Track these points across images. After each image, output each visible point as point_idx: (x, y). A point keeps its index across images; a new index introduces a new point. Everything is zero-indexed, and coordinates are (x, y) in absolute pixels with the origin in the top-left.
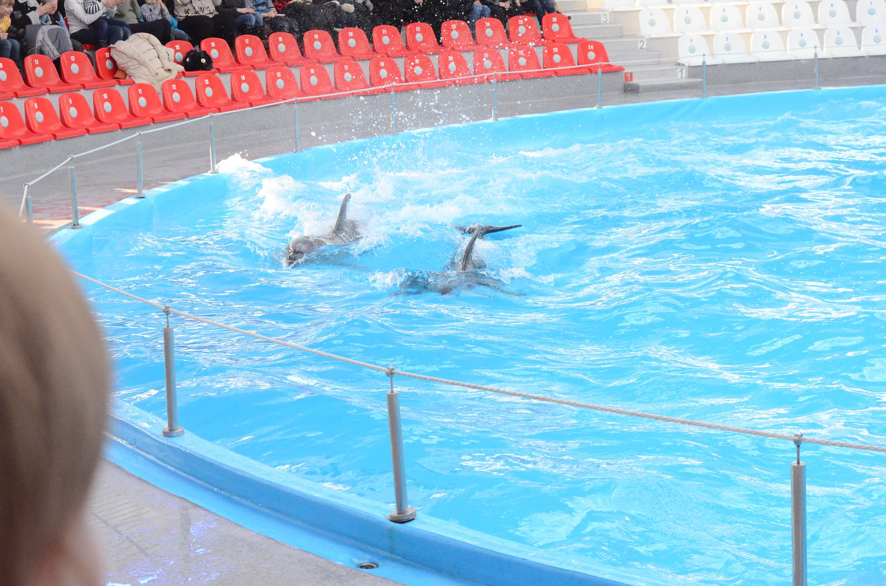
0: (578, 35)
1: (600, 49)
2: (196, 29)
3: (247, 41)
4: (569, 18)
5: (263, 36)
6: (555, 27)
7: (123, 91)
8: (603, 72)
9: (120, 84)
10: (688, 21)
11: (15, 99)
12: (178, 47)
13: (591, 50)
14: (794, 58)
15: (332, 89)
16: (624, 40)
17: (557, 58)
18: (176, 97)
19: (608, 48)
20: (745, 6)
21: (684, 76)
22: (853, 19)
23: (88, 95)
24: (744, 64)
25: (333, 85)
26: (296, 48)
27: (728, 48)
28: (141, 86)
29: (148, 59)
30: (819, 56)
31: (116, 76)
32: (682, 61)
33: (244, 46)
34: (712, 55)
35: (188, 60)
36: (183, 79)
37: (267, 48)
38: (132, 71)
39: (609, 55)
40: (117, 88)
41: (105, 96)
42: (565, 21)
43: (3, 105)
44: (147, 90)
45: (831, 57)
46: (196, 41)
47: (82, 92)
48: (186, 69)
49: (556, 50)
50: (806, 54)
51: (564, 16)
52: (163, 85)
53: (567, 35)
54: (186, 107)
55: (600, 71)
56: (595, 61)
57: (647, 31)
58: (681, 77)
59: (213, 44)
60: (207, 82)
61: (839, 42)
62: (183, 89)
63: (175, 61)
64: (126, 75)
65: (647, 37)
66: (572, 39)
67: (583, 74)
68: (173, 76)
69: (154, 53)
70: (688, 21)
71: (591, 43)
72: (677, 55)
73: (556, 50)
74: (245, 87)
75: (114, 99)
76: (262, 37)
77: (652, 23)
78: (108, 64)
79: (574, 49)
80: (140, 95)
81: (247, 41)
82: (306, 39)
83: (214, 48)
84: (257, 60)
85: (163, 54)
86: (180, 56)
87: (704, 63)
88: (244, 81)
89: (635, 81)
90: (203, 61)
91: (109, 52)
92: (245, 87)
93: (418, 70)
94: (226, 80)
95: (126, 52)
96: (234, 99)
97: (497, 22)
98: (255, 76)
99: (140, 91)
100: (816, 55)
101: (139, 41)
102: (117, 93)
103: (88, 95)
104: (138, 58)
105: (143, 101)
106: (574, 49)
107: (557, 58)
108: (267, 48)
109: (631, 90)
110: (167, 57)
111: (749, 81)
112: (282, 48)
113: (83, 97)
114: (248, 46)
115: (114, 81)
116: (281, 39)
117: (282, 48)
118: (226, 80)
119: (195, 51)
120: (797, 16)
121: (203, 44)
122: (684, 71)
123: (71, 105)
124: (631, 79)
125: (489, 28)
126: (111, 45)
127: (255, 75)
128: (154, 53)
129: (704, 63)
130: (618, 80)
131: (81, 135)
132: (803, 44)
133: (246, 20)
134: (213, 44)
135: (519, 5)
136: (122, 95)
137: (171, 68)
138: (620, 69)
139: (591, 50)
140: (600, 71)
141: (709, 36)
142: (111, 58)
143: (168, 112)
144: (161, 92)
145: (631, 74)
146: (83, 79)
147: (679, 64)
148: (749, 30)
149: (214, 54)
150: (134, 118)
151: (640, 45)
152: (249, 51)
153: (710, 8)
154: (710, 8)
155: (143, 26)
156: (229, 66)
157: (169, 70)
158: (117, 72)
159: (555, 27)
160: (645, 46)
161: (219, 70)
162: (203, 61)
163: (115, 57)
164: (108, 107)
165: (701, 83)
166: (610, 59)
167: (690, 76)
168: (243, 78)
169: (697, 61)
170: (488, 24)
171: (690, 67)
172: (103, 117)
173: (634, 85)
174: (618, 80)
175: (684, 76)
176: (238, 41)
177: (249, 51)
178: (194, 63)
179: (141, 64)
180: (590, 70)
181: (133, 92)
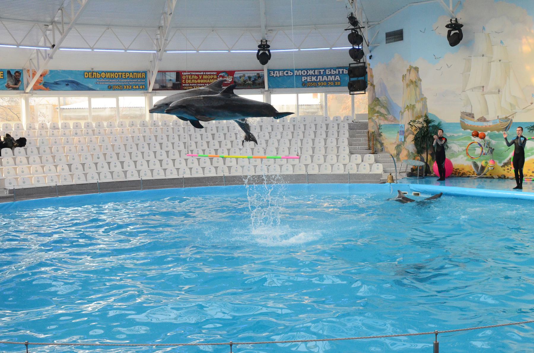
10: (9, 173)
22: (70, 171)
50: (53, 184)
58: (6, 194)
61: (65, 179)
70: (9, 173)
120: (50, 170)
132: (52, 180)
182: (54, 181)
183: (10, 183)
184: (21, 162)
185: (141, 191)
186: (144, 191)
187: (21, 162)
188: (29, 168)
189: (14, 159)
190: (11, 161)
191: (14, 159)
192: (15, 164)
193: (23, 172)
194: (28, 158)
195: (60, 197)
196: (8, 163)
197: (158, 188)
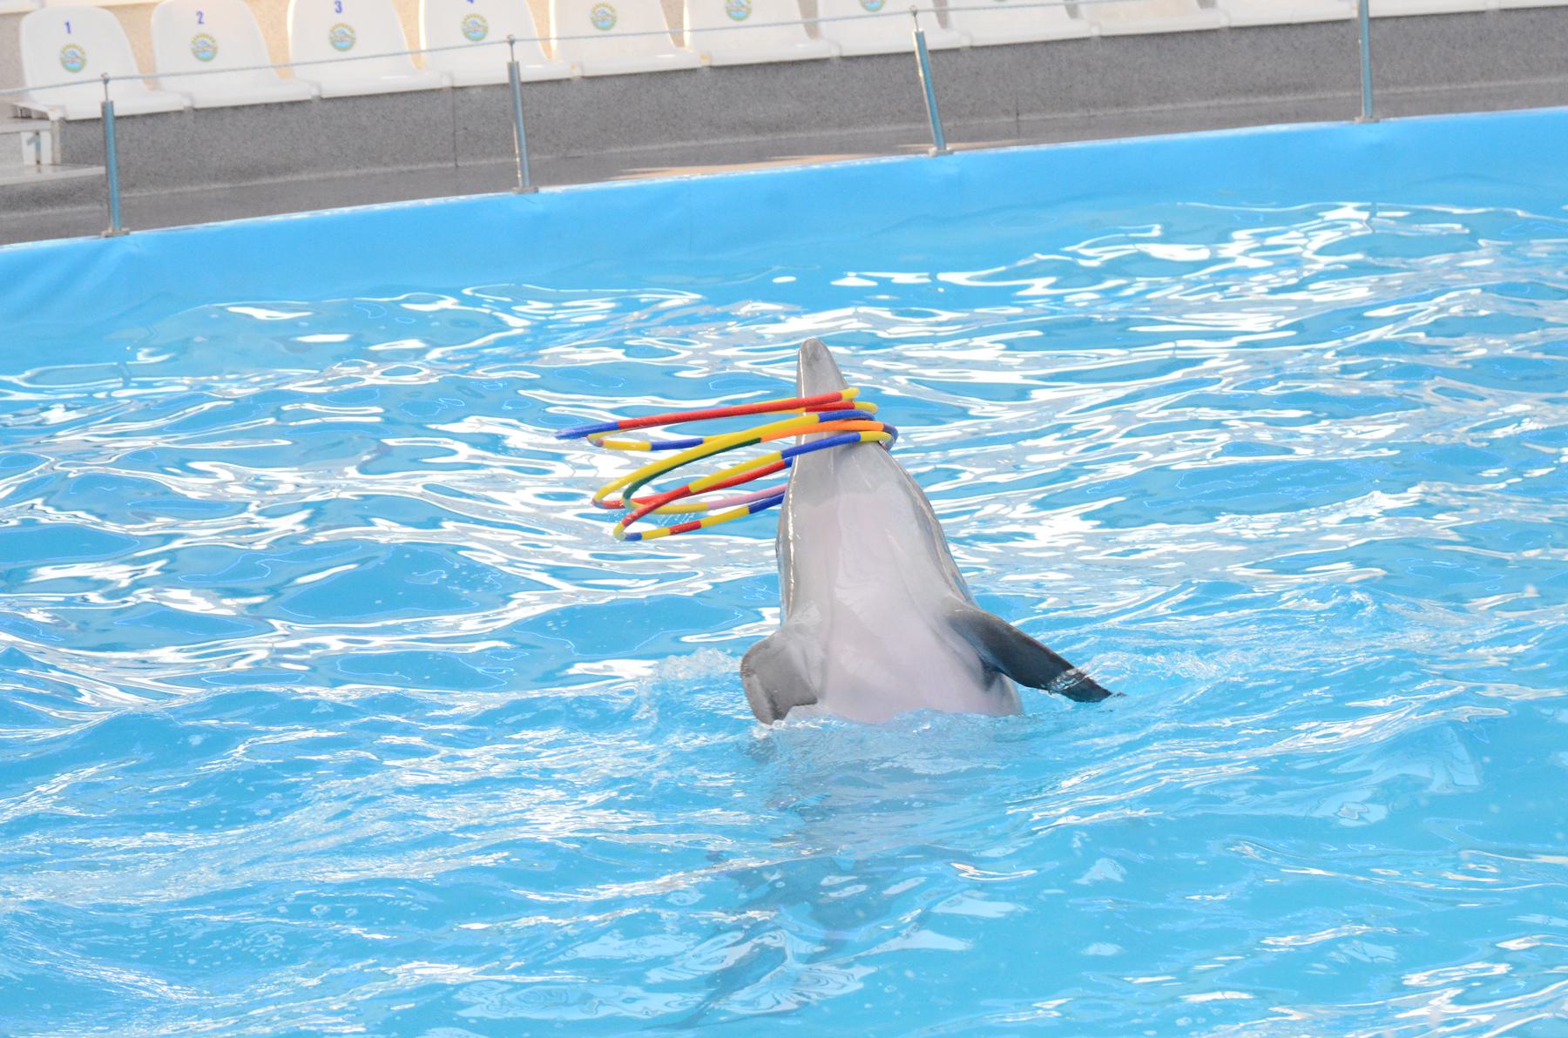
14: (446, 83)
21: (46, 158)
24: (267, 106)
27: (204, 50)
30: (530, 72)
32: (37, 102)
45: (576, 73)
58: (33, 161)
72: (19, 80)
87: (107, 107)
100: (513, 68)
111: (287, 169)
122: (46, 138)
129: (107, 107)
132: (475, 31)
147: (26, 115)
167: (71, 157)
171: (65, 122)
175: (46, 158)
182: (497, 32)
183: (73, 61)
185: (1362, 132)
186: (1391, 127)
195: (544, 190)
197: (1537, 100)
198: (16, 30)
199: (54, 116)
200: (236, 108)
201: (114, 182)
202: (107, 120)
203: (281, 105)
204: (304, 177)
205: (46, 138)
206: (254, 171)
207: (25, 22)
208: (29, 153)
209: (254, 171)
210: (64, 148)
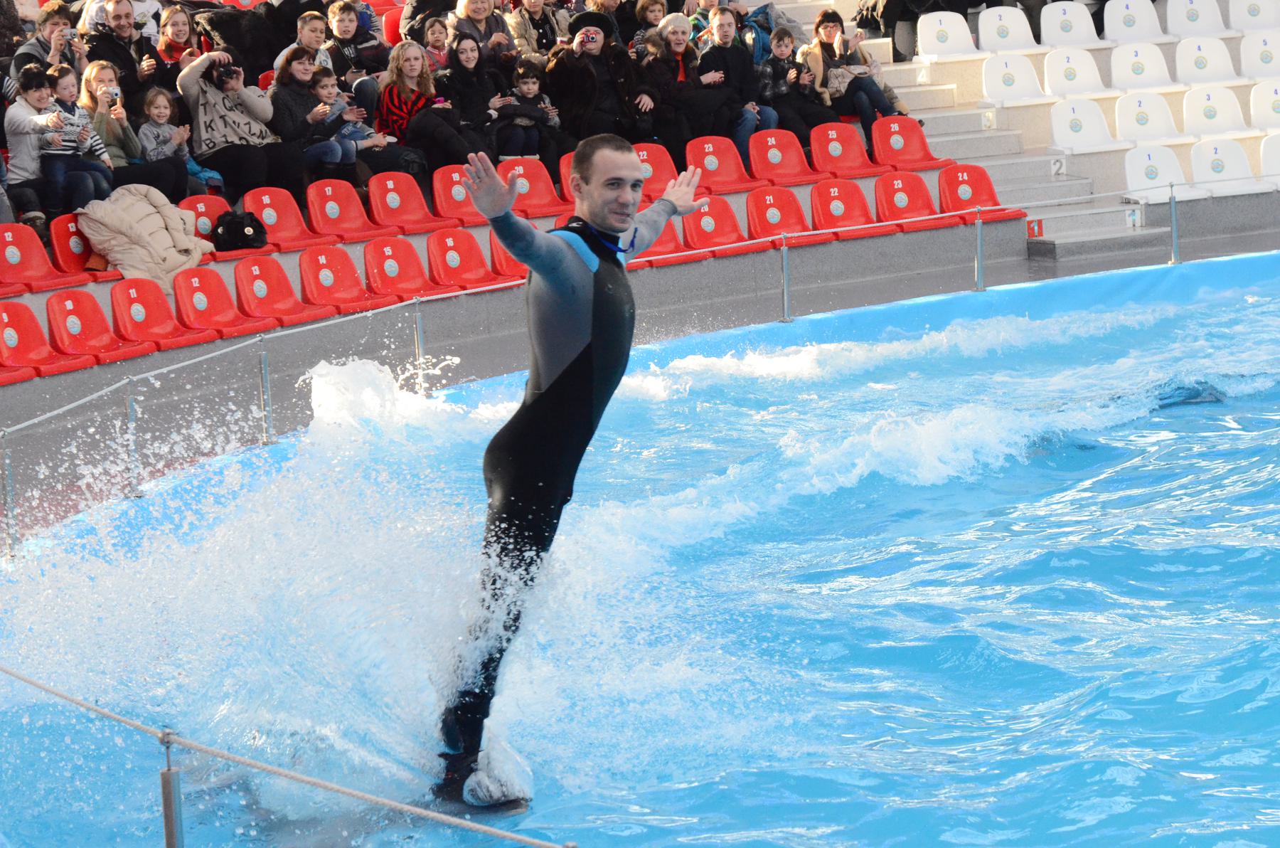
0: (940, 154)
1: (980, 179)
2: (238, 170)
3: (329, 191)
4: (920, 122)
5: (358, 182)
6: (897, 142)
7: (100, 293)
8: (984, 223)
9: (95, 280)
10: (1142, 120)
11: (27, 296)
12: (201, 207)
13: (964, 182)
15: (487, 273)
16: (1025, 160)
17: (901, 199)
18: (200, 301)
19: (993, 176)
20: (1249, 87)
21: (1138, 224)
23: (36, 304)
25: (364, 282)
26: (357, 207)
27: (1218, 167)
28: (136, 283)
29: (149, 232)
31: (89, 265)
32: (1133, 197)
33: (325, 199)
34: (1191, 183)
35: (220, 230)
36: (213, 266)
37: (366, 200)
38: (119, 256)
39: (997, 189)
40: (91, 288)
41: (69, 305)
42: (913, 129)
43: (7, 309)
44: (147, 291)
46: (234, 199)
47: (27, 300)
48: (218, 248)
49: (898, 184)
51: (912, 121)
52: (175, 279)
53: (919, 155)
54: (218, 318)
55: (979, 222)
56: (971, 202)
57: (1066, 141)
58: (1132, 224)
59: (266, 199)
60: (256, 270)
62: (211, 286)
63: (198, 234)
64: (107, 262)
65: (1068, 152)
66: (928, 161)
67: (951, 226)
68: (192, 262)
69: (157, 221)
70: (1142, 120)
71: (966, 168)
73: (898, 184)
74: (326, 277)
75: (86, 309)
76: (356, 184)
77: (1076, 127)
78: (74, 243)
79: (931, 181)
80: (132, 301)
81: (329, 191)
82: (437, 185)
83: (269, 207)
84: (346, 225)
85: (175, 223)
86: (205, 224)
88: (324, 266)
89: (1047, 236)
90: (249, 231)
91: (76, 221)
92: (391, 267)
93: (453, 259)
94: (290, 265)
95: (107, 220)
96: (306, 300)
97: (790, 136)
98: (345, 255)
99: (133, 293)
101: (129, 199)
102: (90, 297)
103: (36, 304)
104: (129, 232)
105: (138, 312)
106: (931, 181)
107: (901, 199)
108: (366, 200)
109: (1040, 255)
110: (181, 227)
112: (393, 200)
113: (26, 309)
114: (331, 202)
115: (86, 275)
116: (390, 184)
117: (393, 200)
118: (290, 265)
119: (233, 215)
121: (248, 203)
122: (1138, 213)
123: (7, 325)
124: (1041, 234)
125: (775, 150)
126: (79, 210)
127: (345, 255)
128: (157, 221)
130: (1015, 234)
131: (30, 378)
133: (325, 153)
134: (266, 199)
135: (829, 103)
136: (99, 300)
137: (190, 246)
138: (1018, 216)
139: (964, 182)
140: (979, 222)
141: (1182, 145)
142: (79, 233)
143: (186, 332)
144: (171, 292)
145: (1040, 222)
146: (29, 273)
147: (1128, 202)
148: (1255, 133)
149: (269, 216)
150: (124, 345)
151: (1054, 169)
152: (332, 209)
153: (1184, 93)
154: (1184, 93)
155: (139, 170)
156: (294, 240)
157: (187, 252)
158: (91, 260)
159: (897, 142)
160: (1063, 170)
161: (278, 247)
162: (249, 231)
163: (87, 232)
164: (74, 324)
165: (1169, 235)
166: (1000, 198)
167: (1151, 222)
168: (322, 260)
169: (1162, 196)
170: (772, 141)
171: (1148, 205)
172: (66, 343)
173: (1044, 243)
174: (1015, 234)
176: (312, 192)
177: (332, 209)
178: (232, 236)
179: (135, 241)
180: (964, 220)
181: (120, 297)
183: (1151, 174)
184: (1200, 64)
187: (1200, 64)
188: (1243, 93)
189: (1169, 51)
190: (1154, 62)
191: (1169, 51)
192: (1174, 77)
193: (1210, 114)
194: (1233, 44)
196: (1138, 69)
198: (1123, 159)
199: (1142, 202)
200: (1234, 197)
201: (1175, 235)
202: (1171, 203)
203: (1257, 195)
204: (1268, 231)
205: (1138, 213)
206: (1243, 228)
207: (1128, 154)
208: (1129, 221)
209: (1243, 228)
210: (1147, 218)
